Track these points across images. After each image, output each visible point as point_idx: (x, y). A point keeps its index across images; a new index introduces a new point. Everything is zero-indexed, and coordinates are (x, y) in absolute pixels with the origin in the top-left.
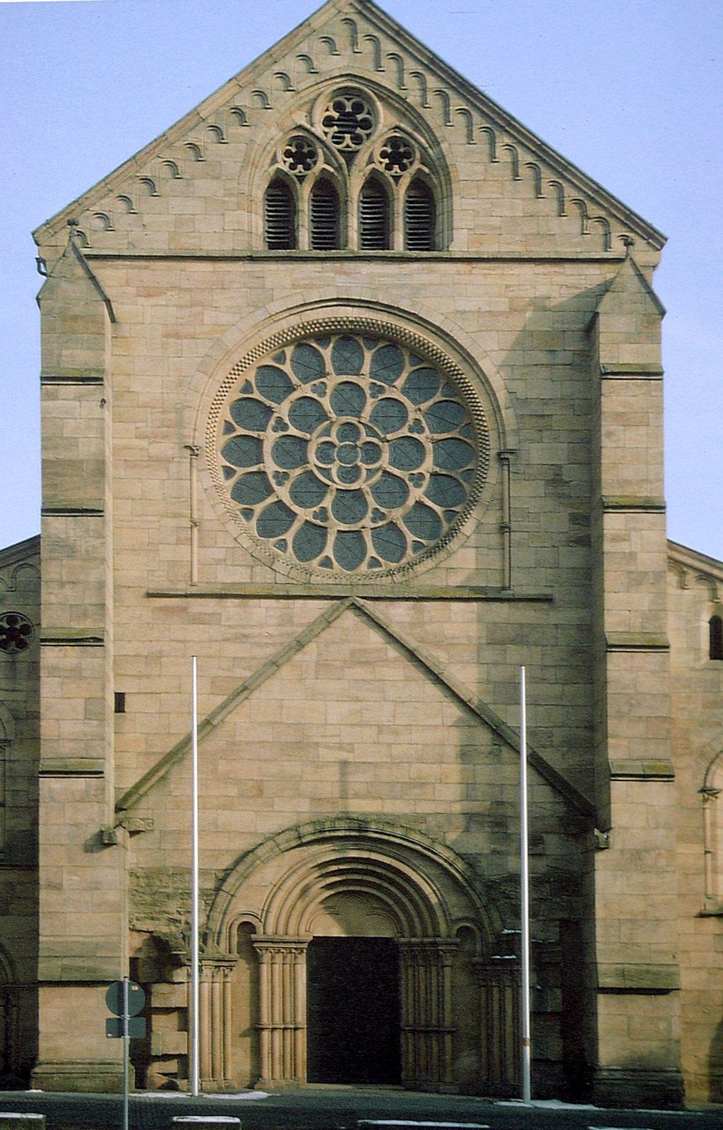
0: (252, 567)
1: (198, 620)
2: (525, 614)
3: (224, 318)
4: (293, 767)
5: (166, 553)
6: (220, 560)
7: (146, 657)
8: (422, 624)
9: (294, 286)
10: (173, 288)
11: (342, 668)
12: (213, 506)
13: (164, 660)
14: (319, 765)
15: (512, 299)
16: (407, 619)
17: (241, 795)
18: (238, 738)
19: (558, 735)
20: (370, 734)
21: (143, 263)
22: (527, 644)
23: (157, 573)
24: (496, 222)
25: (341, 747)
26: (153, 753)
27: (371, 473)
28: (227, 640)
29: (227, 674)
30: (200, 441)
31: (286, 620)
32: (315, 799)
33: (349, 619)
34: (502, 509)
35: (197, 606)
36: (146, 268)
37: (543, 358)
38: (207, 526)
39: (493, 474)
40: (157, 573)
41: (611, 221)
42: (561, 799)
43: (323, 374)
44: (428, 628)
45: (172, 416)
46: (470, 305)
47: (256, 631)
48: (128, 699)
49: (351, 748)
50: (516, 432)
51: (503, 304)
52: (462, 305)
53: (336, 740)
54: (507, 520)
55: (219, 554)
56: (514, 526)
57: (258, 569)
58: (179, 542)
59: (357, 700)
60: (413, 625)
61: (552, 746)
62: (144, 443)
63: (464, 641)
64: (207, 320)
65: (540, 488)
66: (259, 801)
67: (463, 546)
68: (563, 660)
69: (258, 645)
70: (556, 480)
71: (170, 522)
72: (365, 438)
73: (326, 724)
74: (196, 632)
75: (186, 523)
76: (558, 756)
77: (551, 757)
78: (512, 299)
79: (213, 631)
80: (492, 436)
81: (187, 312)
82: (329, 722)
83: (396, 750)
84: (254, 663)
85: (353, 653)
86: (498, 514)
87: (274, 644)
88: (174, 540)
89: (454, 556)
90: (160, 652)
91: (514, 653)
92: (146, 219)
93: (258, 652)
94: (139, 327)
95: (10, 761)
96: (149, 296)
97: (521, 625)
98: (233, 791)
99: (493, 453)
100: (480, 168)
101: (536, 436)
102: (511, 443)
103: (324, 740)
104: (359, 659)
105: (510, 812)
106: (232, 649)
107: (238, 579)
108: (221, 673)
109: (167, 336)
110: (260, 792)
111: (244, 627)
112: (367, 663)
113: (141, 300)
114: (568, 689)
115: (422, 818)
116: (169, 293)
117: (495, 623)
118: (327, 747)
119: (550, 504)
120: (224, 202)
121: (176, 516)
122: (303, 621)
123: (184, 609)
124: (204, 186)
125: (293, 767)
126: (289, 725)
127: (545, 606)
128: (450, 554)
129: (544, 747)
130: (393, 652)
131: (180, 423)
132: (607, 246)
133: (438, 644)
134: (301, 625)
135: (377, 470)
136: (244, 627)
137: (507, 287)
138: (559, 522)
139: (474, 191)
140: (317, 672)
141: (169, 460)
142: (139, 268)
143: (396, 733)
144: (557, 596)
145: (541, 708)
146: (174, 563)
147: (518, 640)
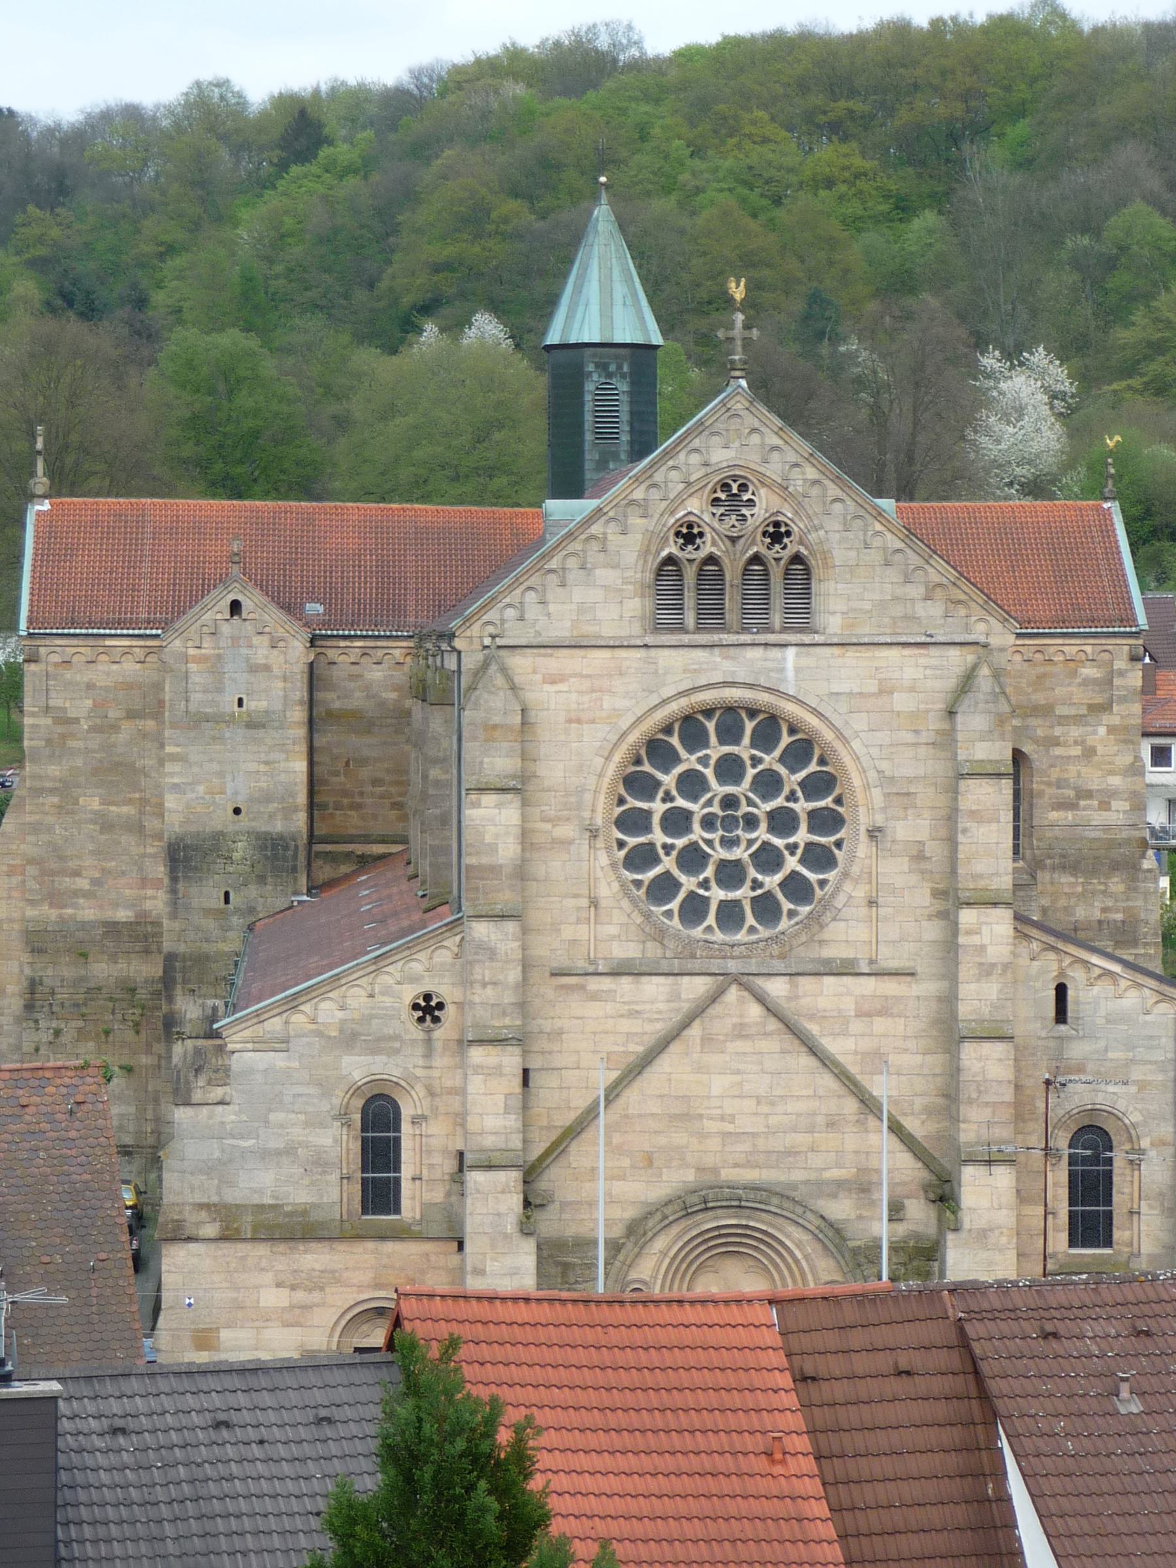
0: (644, 942)
1: (595, 997)
2: (890, 987)
3: (621, 703)
4: (680, 1138)
5: (568, 932)
6: (614, 936)
7: (549, 1034)
8: (797, 997)
9: (685, 671)
10: (576, 675)
11: (725, 1041)
12: (609, 884)
13: (564, 1036)
14: (703, 1135)
15: (881, 681)
16: (784, 993)
17: (633, 1167)
18: (630, 1112)
19: (919, 1102)
20: (749, 1105)
21: (549, 651)
22: (892, 1015)
23: (559, 952)
24: (867, 606)
25: (722, 1118)
26: (555, 1127)
27: (750, 842)
28: (622, 1016)
29: (622, 1049)
30: (599, 821)
31: (675, 997)
32: (700, 1169)
33: (733, 993)
34: (870, 883)
35: (594, 984)
36: (551, 655)
37: (910, 737)
38: (603, 903)
39: (863, 848)
40: (559, 952)
41: (973, 605)
42: (920, 1165)
43: (706, 745)
44: (803, 1001)
45: (573, 799)
46: (844, 687)
47: (648, 1007)
48: (531, 1074)
49: (732, 1119)
50: (884, 809)
51: (872, 687)
52: (836, 687)
53: (719, 1111)
54: (874, 895)
55: (613, 930)
56: (880, 900)
57: (649, 945)
58: (579, 921)
59: (738, 1072)
60: (789, 999)
61: (912, 1114)
62: (548, 826)
63: (835, 1014)
64: (606, 705)
65: (904, 863)
66: (650, 1171)
67: (834, 919)
68: (924, 1031)
69: (651, 1021)
70: (920, 857)
71: (571, 903)
72: (745, 809)
73: (709, 1097)
74: (594, 1009)
75: (584, 902)
76: (917, 1123)
77: (912, 1125)
78: (881, 681)
79: (610, 1008)
80: (862, 810)
81: (586, 698)
82: (713, 1094)
83: (773, 1120)
84: (646, 1038)
85: (734, 1026)
86: (867, 887)
87: (663, 1019)
88: (573, 919)
89: (826, 929)
90: (561, 1028)
91: (881, 1025)
92: (552, 608)
93: (649, 1028)
94: (545, 712)
95: (427, 1136)
96: (553, 682)
97: (886, 997)
98: (626, 1162)
99: (863, 829)
100: (853, 554)
101: (901, 813)
102: (879, 820)
103: (708, 1112)
104: (741, 1032)
105: (875, 1179)
106: (626, 1025)
107: (631, 954)
108: (616, 1048)
109: (570, 721)
110: (650, 1162)
111: (636, 1003)
112: (746, 1037)
113: (547, 687)
114: (929, 1058)
115: (794, 1186)
116: (572, 680)
117: (863, 996)
118: (711, 1119)
119: (913, 879)
120: (622, 590)
121: (576, 896)
122: (691, 996)
123: (582, 987)
124: (604, 575)
125: (680, 1138)
126: (677, 1098)
127: (909, 978)
128: (822, 927)
129: (905, 1114)
130: (773, 1025)
131: (579, 806)
132: (967, 629)
133: (812, 1017)
134: (688, 1000)
135: (756, 839)
136: (636, 1003)
137: (877, 669)
138: (922, 898)
139: (848, 576)
140: (702, 1046)
141: (571, 842)
142: (544, 656)
143: (773, 1104)
144: (919, 970)
145: (904, 1078)
146: (573, 942)
147: (884, 1012)
